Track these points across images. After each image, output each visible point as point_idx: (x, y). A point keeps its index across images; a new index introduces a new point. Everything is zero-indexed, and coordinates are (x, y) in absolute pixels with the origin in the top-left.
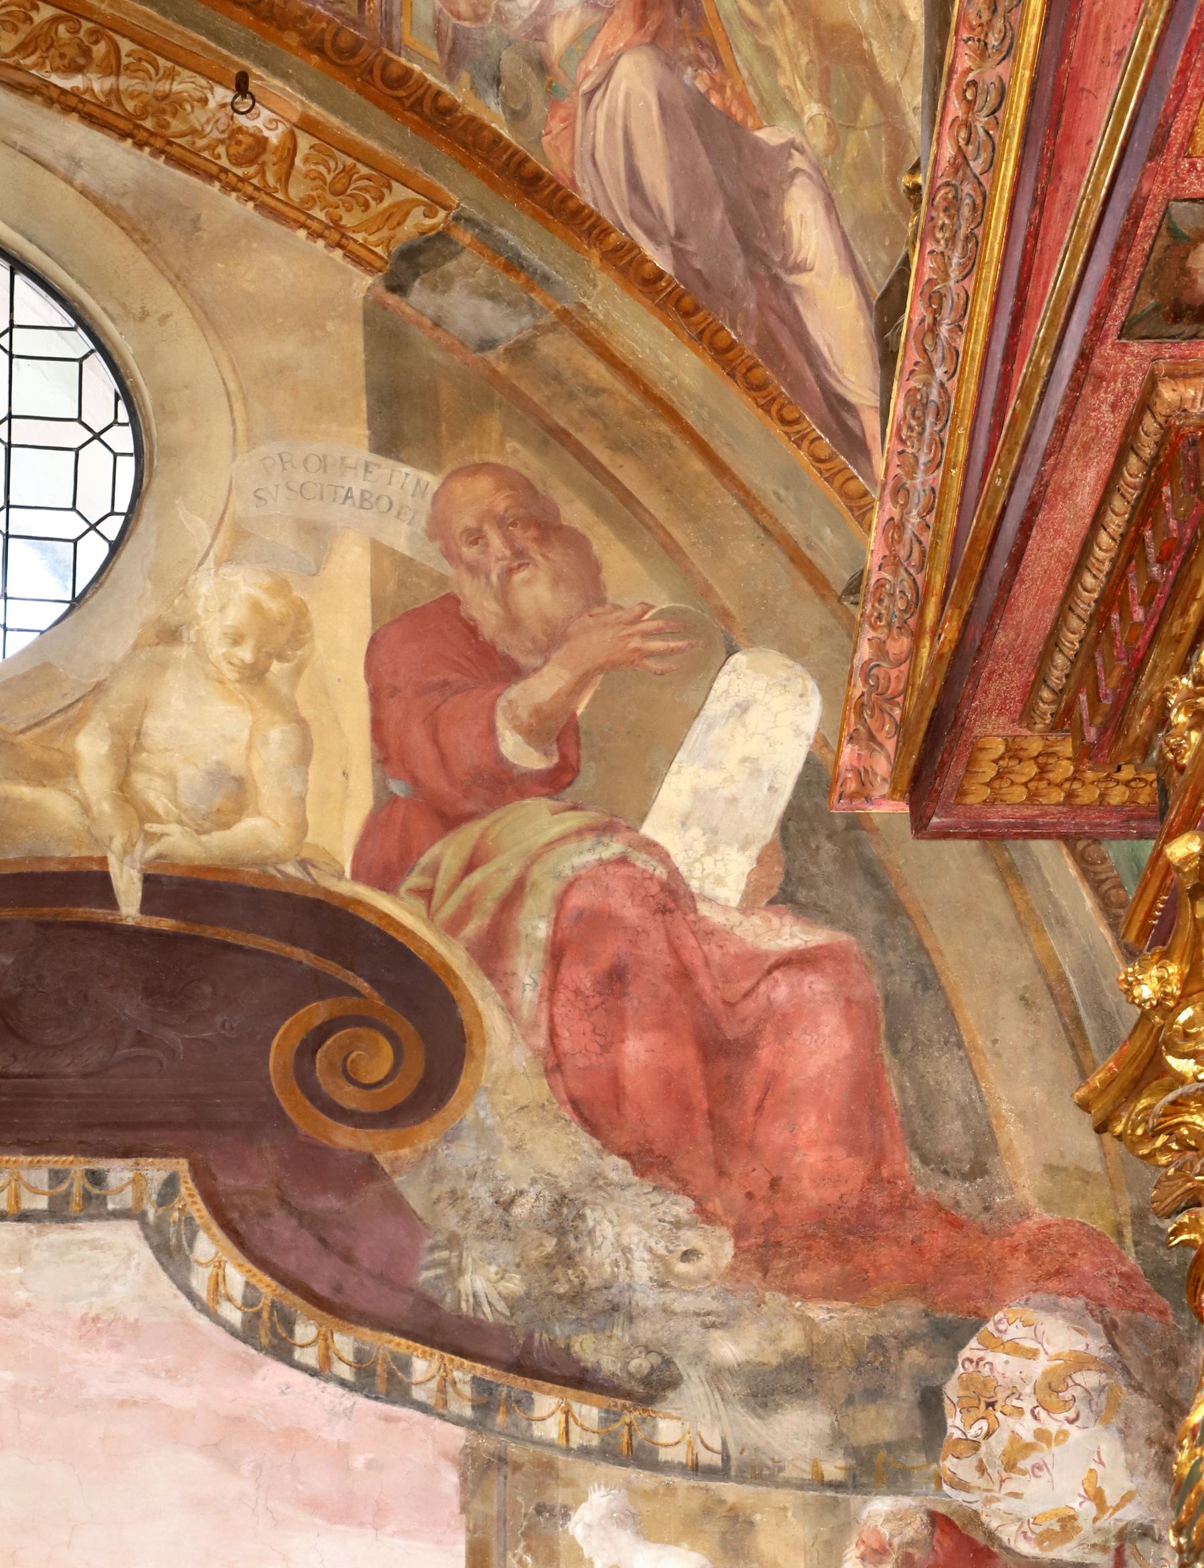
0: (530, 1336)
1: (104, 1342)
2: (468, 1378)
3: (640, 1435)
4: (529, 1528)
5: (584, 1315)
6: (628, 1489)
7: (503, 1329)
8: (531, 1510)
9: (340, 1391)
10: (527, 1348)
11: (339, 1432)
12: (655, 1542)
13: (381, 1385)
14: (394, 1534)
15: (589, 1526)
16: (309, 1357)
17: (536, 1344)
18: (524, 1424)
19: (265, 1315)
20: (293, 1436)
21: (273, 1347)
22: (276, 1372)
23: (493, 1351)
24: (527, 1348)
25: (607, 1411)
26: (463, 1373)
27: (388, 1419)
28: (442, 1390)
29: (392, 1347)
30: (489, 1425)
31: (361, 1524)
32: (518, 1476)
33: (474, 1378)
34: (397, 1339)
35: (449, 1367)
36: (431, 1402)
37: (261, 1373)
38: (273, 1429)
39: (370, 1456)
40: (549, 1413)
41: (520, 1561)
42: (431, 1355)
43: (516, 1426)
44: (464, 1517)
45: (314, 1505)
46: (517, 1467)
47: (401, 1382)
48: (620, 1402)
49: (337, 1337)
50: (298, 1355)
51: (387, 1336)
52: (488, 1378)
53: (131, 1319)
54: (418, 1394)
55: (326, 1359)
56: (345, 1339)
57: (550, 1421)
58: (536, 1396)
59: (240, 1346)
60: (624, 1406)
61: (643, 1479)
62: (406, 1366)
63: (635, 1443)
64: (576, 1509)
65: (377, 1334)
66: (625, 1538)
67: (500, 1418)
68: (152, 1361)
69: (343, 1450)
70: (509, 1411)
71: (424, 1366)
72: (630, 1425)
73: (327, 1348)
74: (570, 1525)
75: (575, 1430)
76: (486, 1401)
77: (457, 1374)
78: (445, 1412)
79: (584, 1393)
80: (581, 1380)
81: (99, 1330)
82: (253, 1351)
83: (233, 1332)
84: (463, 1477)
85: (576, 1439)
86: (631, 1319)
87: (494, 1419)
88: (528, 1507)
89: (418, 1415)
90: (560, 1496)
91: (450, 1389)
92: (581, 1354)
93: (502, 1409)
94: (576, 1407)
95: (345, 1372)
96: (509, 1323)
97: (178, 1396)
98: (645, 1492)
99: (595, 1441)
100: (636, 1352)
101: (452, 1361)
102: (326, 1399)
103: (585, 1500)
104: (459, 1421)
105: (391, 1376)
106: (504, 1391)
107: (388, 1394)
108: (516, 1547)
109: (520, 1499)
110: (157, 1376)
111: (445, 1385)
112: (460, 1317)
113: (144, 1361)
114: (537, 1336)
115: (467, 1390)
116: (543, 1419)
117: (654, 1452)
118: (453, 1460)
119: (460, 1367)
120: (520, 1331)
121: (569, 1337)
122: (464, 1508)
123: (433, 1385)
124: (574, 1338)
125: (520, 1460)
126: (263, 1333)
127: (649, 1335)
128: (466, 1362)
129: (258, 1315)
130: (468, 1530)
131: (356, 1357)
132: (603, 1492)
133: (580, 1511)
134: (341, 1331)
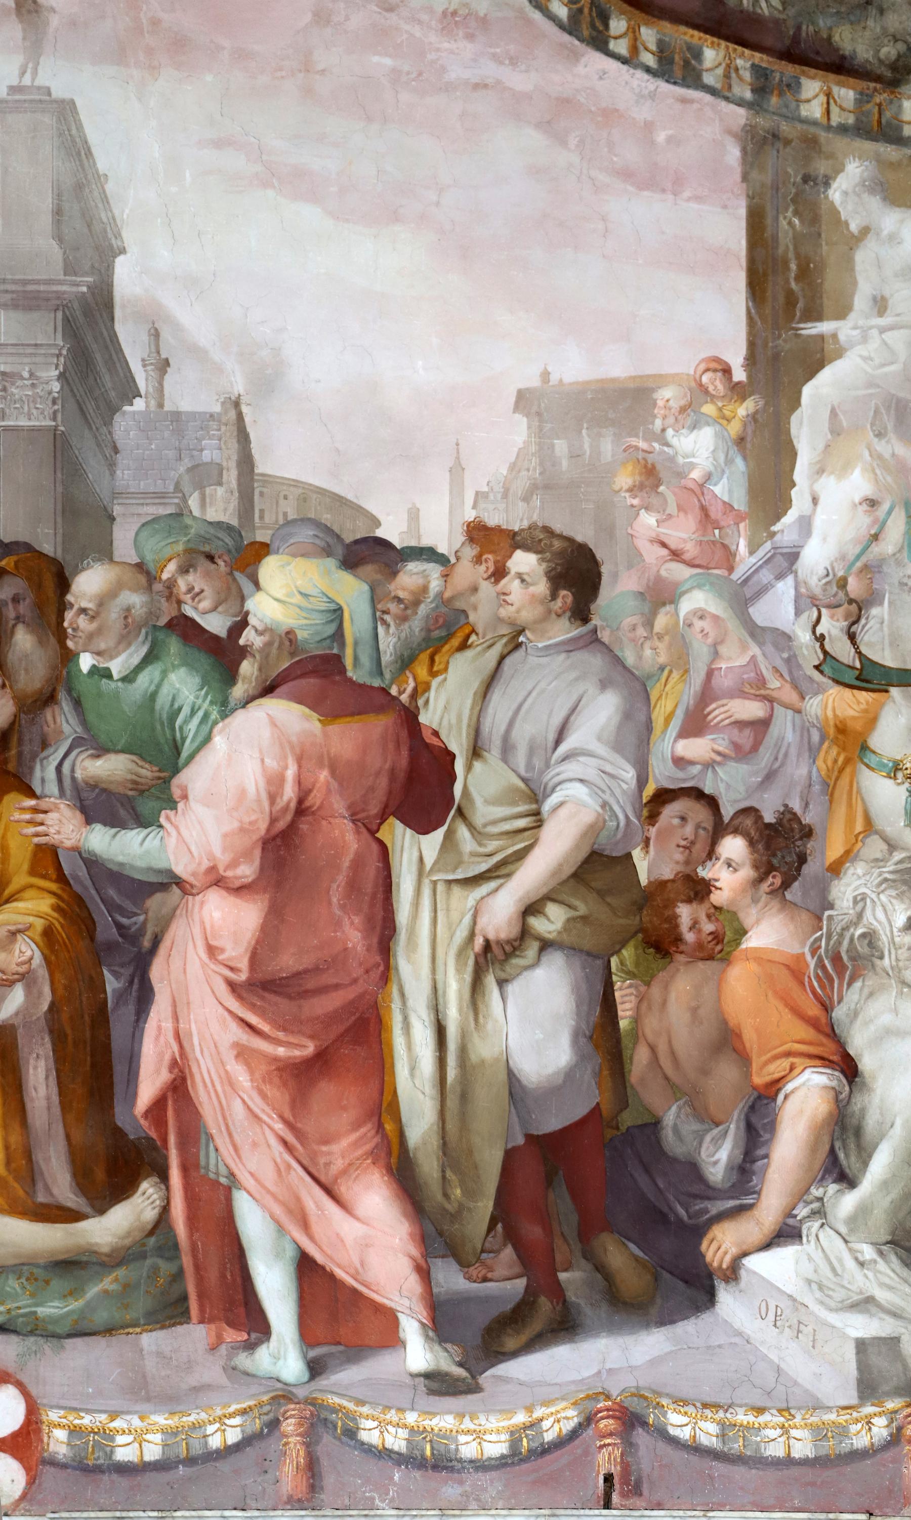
0: (799, 28)
1: (461, 33)
2: (748, 65)
3: (888, 115)
4: (797, 194)
5: (843, 9)
6: (878, 161)
7: (777, 22)
8: (799, 179)
9: (646, 76)
10: (796, 39)
11: (643, 113)
12: (899, 206)
13: (678, 72)
14: (689, 200)
15: (845, 193)
16: (621, 47)
17: (804, 34)
18: (793, 105)
19: (586, 11)
20: (610, 115)
21: (593, 38)
22: (595, 60)
23: (769, 42)
24: (796, 39)
25: (861, 94)
26: (745, 61)
27: (684, 101)
28: (727, 76)
29: (687, 38)
30: (765, 106)
31: (664, 191)
32: (788, 150)
33: (753, 65)
34: (691, 31)
35: (733, 55)
36: (718, 86)
37: (583, 60)
38: (593, 109)
39: (671, 132)
40: (815, 97)
41: (790, 223)
42: (719, 45)
43: (787, 106)
44: (744, 185)
45: (626, 174)
46: (787, 142)
47: (694, 69)
48: (872, 85)
49: (643, 30)
50: (612, 45)
51: (683, 28)
52: (764, 65)
53: (482, 14)
54: (709, 79)
55: (634, 49)
56: (650, 31)
57: (815, 103)
58: (804, 81)
59: (566, 38)
60: (875, 90)
61: (890, 152)
62: (698, 55)
63: (883, 121)
64: (835, 178)
65: (675, 27)
66: (874, 203)
67: (774, 100)
68: (498, 50)
69: (649, 127)
70: (781, 94)
71: (712, 54)
72: (880, 105)
73: (635, 39)
74: (830, 192)
75: (834, 110)
76: (763, 85)
77: (739, 62)
78: (729, 95)
79: (842, 78)
80: (839, 66)
81: (456, 22)
82: (577, 42)
83: (561, 26)
84: (744, 151)
85: (836, 118)
86: (882, 11)
87: (769, 101)
88: (796, 176)
89: (708, 98)
90: (821, 167)
91: (733, 75)
92: (840, 44)
93: (776, 92)
94: (835, 90)
95: (649, 59)
96: (782, 16)
97: (519, 80)
98: (891, 164)
99: (851, 120)
100: (886, 41)
101: (735, 50)
102: (635, 83)
103: (842, 170)
104: (740, 103)
105: (687, 63)
106: (777, 76)
107: (684, 79)
108: (787, 210)
109: (789, 170)
110: (501, 63)
111: (730, 70)
112: (742, 12)
113: (492, 50)
114: (804, 27)
115: (747, 75)
116: (808, 101)
117: (899, 129)
118: (735, 136)
119: (742, 55)
120: (791, 23)
121: (830, 29)
122: (745, 178)
123: (720, 71)
124: (834, 29)
125: (790, 137)
126: (584, 26)
127: (897, 25)
128: (747, 52)
129: (580, 11)
130: (748, 196)
131: (658, 47)
132: (857, 164)
133: (838, 180)
134: (646, 24)
